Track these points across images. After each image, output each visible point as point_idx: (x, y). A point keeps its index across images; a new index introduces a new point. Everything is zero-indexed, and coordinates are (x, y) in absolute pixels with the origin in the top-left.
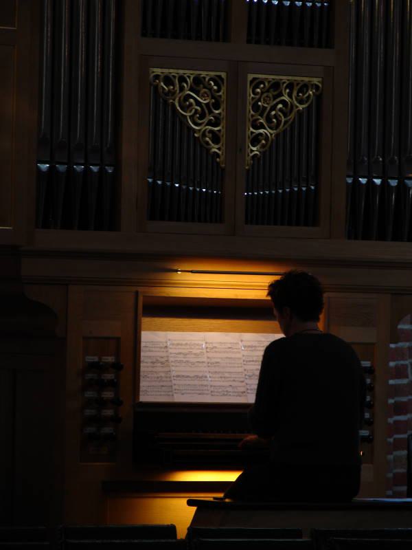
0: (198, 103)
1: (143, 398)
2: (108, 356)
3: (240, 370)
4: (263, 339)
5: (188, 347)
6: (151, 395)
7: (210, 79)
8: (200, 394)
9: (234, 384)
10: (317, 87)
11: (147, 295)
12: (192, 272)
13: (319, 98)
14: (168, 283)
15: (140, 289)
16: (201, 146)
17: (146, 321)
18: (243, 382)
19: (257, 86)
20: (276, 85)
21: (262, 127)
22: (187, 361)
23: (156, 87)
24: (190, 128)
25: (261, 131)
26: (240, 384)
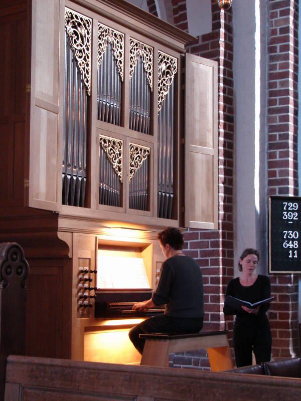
0: (114, 153)
1: (100, 286)
7: (118, 143)
10: (148, 151)
12: (121, 228)
13: (149, 156)
15: (97, 236)
16: (115, 173)
19: (131, 149)
20: (137, 149)
21: (133, 166)
23: (101, 143)
24: (111, 164)
25: (132, 168)
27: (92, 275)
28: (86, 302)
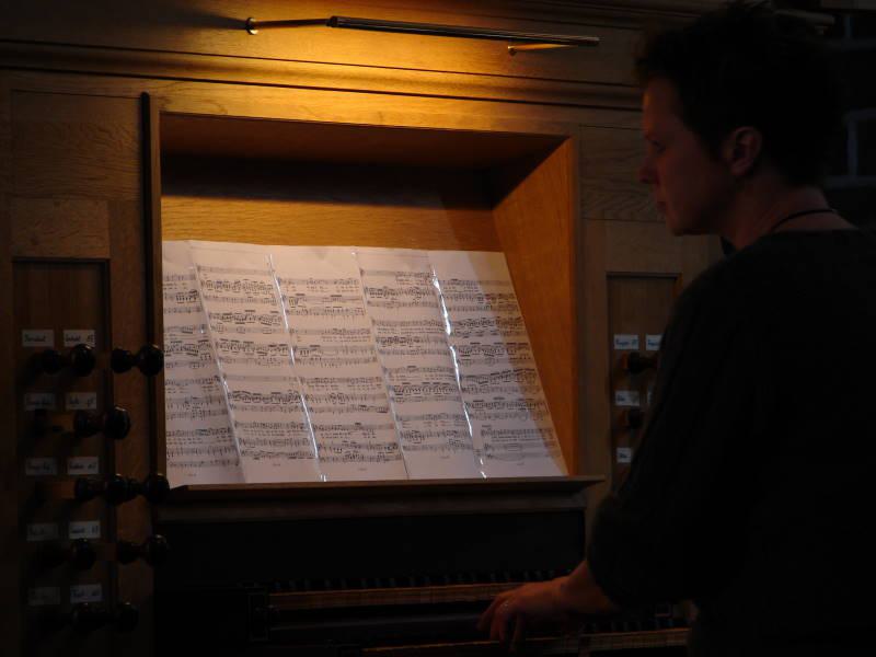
1: (187, 468)
2: (78, 327)
3: (372, 370)
4: (406, 269)
5: (242, 294)
6: (182, 465)
8: (292, 456)
9: (366, 418)
11: (172, 108)
14: (191, 67)
15: (155, 88)
17: (173, 209)
18: (385, 410)
22: (248, 343)
26: (382, 419)
27: (129, 384)
28: (88, 593)
